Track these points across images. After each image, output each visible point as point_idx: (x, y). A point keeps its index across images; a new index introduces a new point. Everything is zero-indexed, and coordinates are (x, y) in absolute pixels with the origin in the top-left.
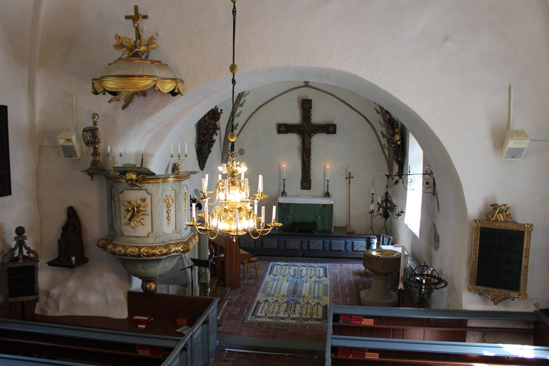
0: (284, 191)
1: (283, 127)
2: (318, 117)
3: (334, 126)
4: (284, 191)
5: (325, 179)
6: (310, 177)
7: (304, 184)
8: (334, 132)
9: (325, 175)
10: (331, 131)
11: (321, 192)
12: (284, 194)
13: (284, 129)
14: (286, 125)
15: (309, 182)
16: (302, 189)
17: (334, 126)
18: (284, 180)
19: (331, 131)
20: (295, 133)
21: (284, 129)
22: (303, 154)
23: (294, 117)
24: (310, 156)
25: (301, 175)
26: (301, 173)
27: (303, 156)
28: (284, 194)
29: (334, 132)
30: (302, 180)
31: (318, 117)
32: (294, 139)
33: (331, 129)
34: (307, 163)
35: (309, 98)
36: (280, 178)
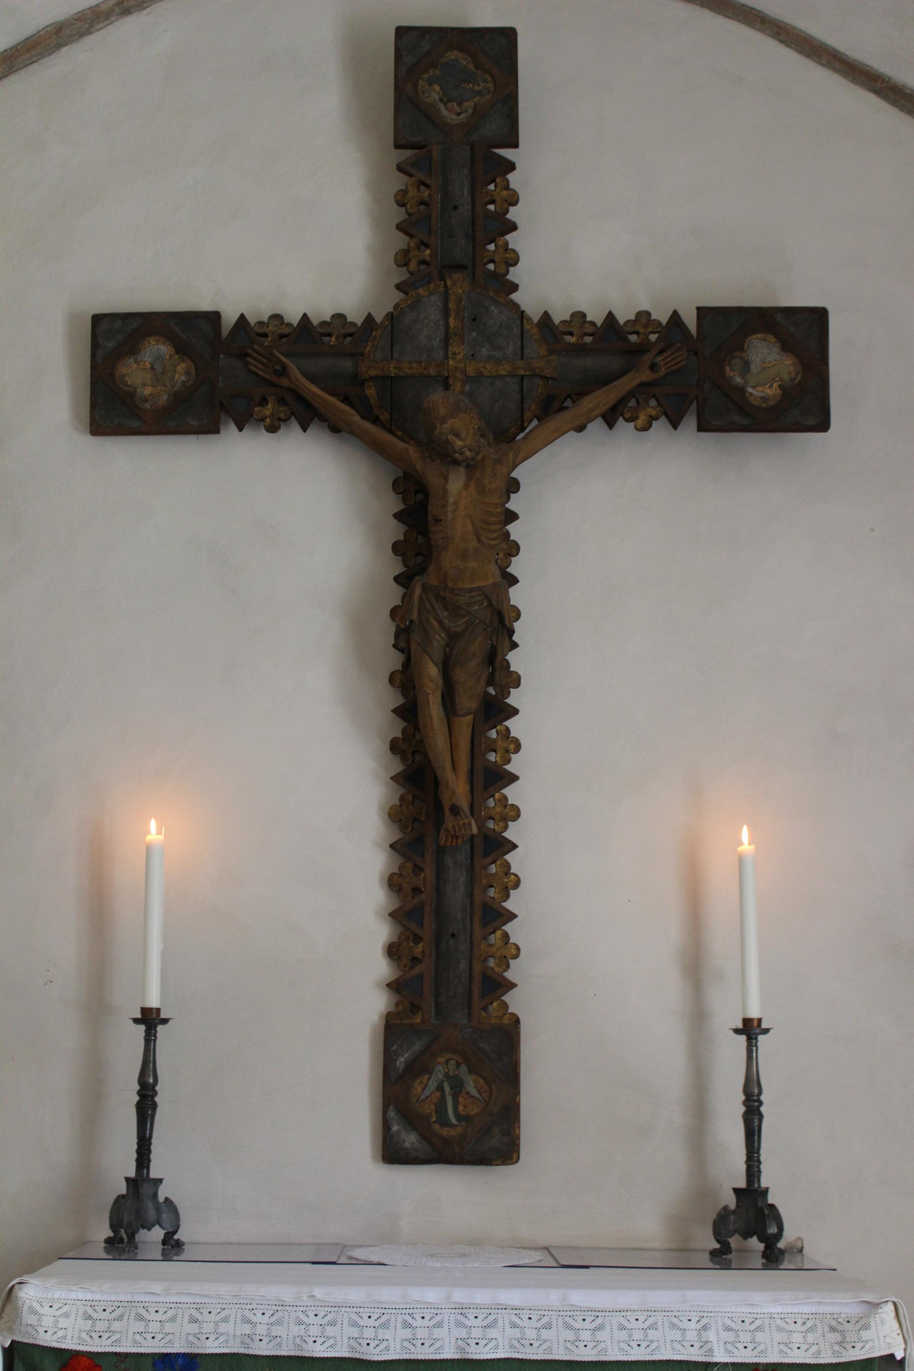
0: (141, 1184)
1: (156, 349)
2: (588, 242)
3: (804, 332)
4: (141, 1184)
5: (698, 1018)
6: (499, 986)
7: (425, 1090)
8: (804, 406)
9: (695, 967)
10: (762, 391)
11: (648, 1196)
12: (138, 1221)
13: (170, 375)
14: (190, 330)
15: (497, 1053)
16: (392, 1153)
17: (804, 332)
18: (150, 1020)
19: (762, 391)
20: (307, 414)
21: (170, 375)
22: (405, 680)
23: (310, 244)
24: (497, 710)
25: (381, 968)
26: (382, 932)
27: (409, 712)
28: (138, 1221)
29: (804, 406)
30: (393, 1030)
31: (588, 242)
32: (299, 511)
33: (765, 367)
34: (457, 787)
35: (484, 16)
36: (96, 1005)
